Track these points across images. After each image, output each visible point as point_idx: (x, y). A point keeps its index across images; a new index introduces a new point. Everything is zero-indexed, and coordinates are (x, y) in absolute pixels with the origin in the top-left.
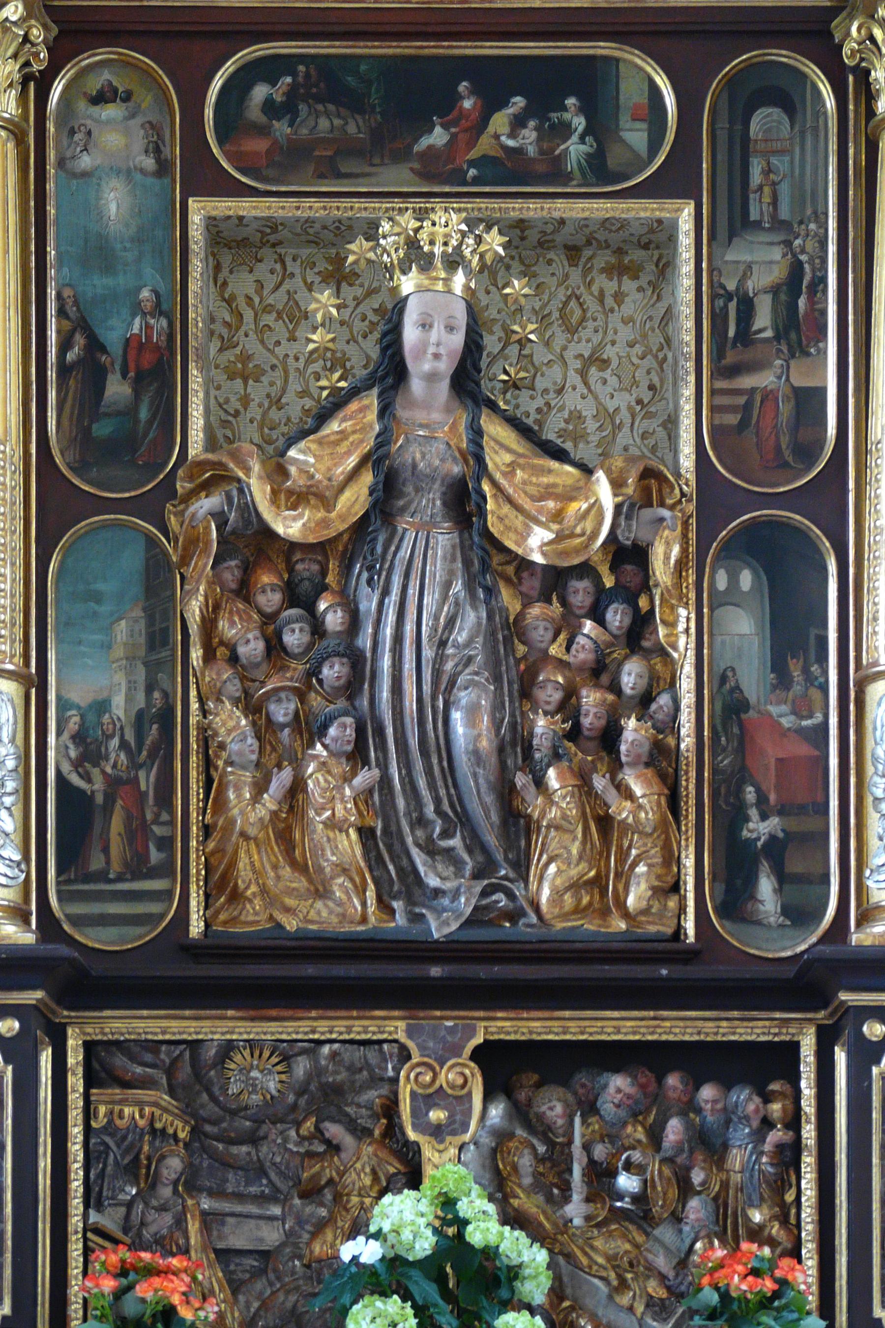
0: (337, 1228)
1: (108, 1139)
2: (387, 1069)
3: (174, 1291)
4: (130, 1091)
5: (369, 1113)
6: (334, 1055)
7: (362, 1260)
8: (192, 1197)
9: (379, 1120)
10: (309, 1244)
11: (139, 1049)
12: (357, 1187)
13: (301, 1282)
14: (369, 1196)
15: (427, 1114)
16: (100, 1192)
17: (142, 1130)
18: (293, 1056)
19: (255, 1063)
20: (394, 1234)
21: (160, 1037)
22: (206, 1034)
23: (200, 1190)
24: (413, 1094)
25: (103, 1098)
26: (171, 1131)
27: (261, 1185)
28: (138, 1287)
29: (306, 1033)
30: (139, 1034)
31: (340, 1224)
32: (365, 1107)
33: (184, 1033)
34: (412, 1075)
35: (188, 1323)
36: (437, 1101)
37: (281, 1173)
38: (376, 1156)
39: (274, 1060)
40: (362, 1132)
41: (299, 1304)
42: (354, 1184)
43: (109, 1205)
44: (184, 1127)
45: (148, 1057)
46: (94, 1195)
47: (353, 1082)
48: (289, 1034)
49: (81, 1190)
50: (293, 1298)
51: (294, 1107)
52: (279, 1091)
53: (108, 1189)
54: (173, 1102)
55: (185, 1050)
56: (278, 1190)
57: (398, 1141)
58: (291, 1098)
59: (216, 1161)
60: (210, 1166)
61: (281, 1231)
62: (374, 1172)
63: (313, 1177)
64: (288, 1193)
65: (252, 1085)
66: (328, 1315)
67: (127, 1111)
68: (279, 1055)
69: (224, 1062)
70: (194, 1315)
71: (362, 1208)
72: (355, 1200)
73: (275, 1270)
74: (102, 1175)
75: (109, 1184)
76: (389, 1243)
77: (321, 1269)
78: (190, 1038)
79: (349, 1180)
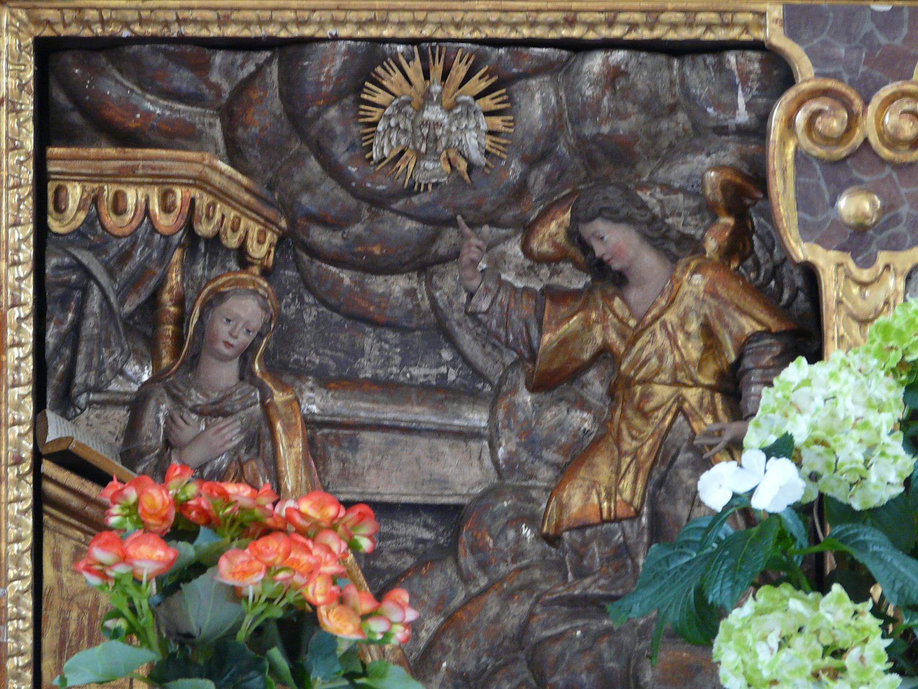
0: (622, 454)
1: (86, 258)
2: (735, 107)
3: (311, 572)
4: (140, 152)
5: (692, 203)
6: (614, 75)
7: (759, 503)
8: (284, 387)
9: (715, 218)
10: (554, 490)
11: (160, 59)
12: (669, 361)
13: (537, 574)
14: (697, 384)
15: (833, 203)
16: (70, 375)
17: (167, 237)
18: (518, 77)
19: (436, 88)
20: (820, 449)
21: (215, 31)
22: (321, 24)
23: (300, 373)
24: (801, 158)
25: (76, 167)
26: (232, 242)
27: (438, 365)
28: (224, 563)
29: (553, 25)
30: (166, 24)
31: (629, 444)
32: (681, 190)
33: (270, 21)
34: (801, 118)
35: (342, 648)
36: (856, 174)
37: (488, 337)
38: (715, 295)
39: (478, 84)
40: (678, 244)
41: (534, 622)
42: (661, 358)
43: (89, 403)
44: (262, 234)
45: (183, 79)
46: (53, 382)
47: (655, 137)
48: (514, 26)
49: (29, 366)
50: (518, 610)
51: (520, 190)
52: (487, 153)
53: (88, 368)
54: (240, 177)
55: (268, 61)
56: (479, 375)
57: (757, 266)
58: (515, 170)
59: (334, 309)
60: (320, 321)
61: (488, 462)
62: (708, 332)
63: (564, 342)
64: (503, 379)
65: (426, 138)
66: (604, 645)
67: (132, 196)
68: (489, 73)
69: (360, 89)
70: (360, 630)
71: (680, 409)
72: (662, 392)
73: (476, 548)
74: (73, 336)
75: (90, 355)
76: (806, 470)
77: (585, 544)
78: (283, 34)
79: (650, 349)
